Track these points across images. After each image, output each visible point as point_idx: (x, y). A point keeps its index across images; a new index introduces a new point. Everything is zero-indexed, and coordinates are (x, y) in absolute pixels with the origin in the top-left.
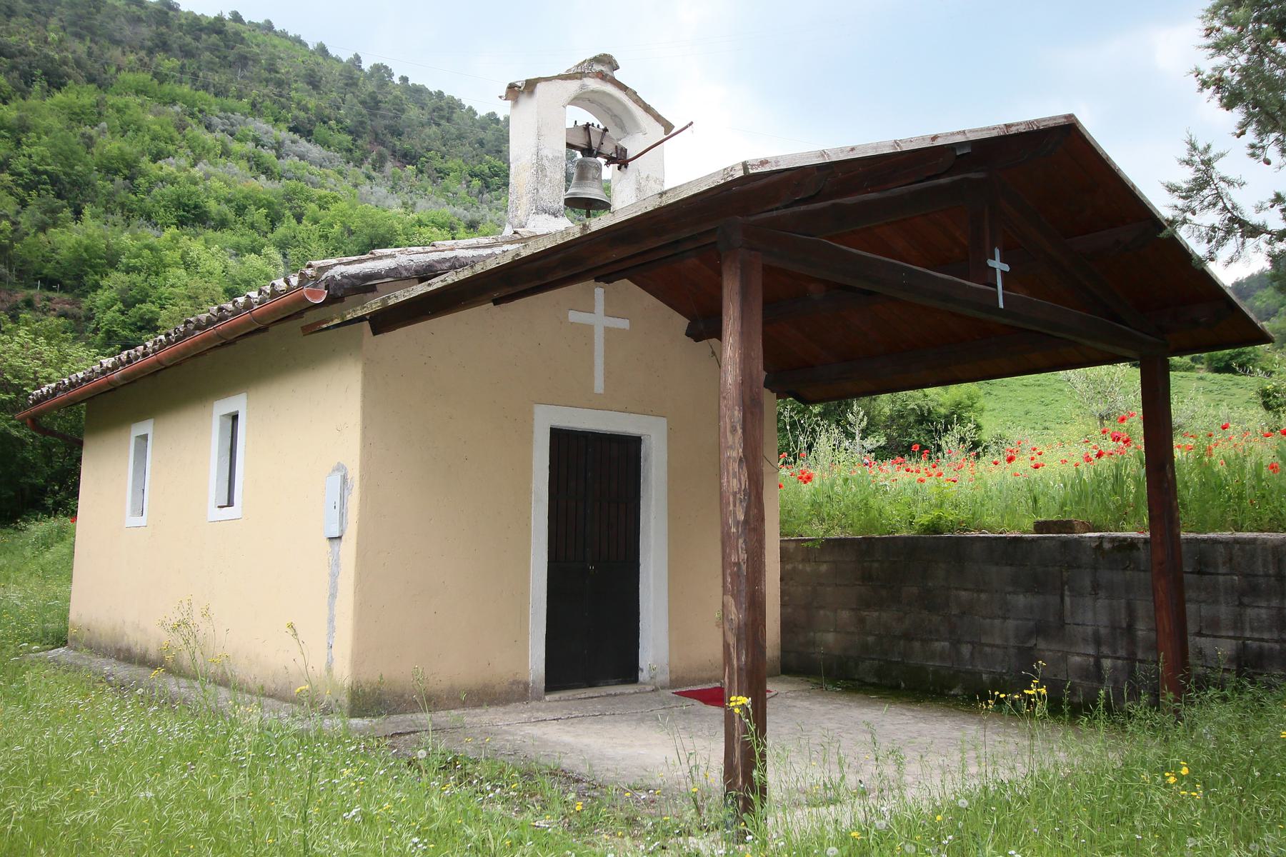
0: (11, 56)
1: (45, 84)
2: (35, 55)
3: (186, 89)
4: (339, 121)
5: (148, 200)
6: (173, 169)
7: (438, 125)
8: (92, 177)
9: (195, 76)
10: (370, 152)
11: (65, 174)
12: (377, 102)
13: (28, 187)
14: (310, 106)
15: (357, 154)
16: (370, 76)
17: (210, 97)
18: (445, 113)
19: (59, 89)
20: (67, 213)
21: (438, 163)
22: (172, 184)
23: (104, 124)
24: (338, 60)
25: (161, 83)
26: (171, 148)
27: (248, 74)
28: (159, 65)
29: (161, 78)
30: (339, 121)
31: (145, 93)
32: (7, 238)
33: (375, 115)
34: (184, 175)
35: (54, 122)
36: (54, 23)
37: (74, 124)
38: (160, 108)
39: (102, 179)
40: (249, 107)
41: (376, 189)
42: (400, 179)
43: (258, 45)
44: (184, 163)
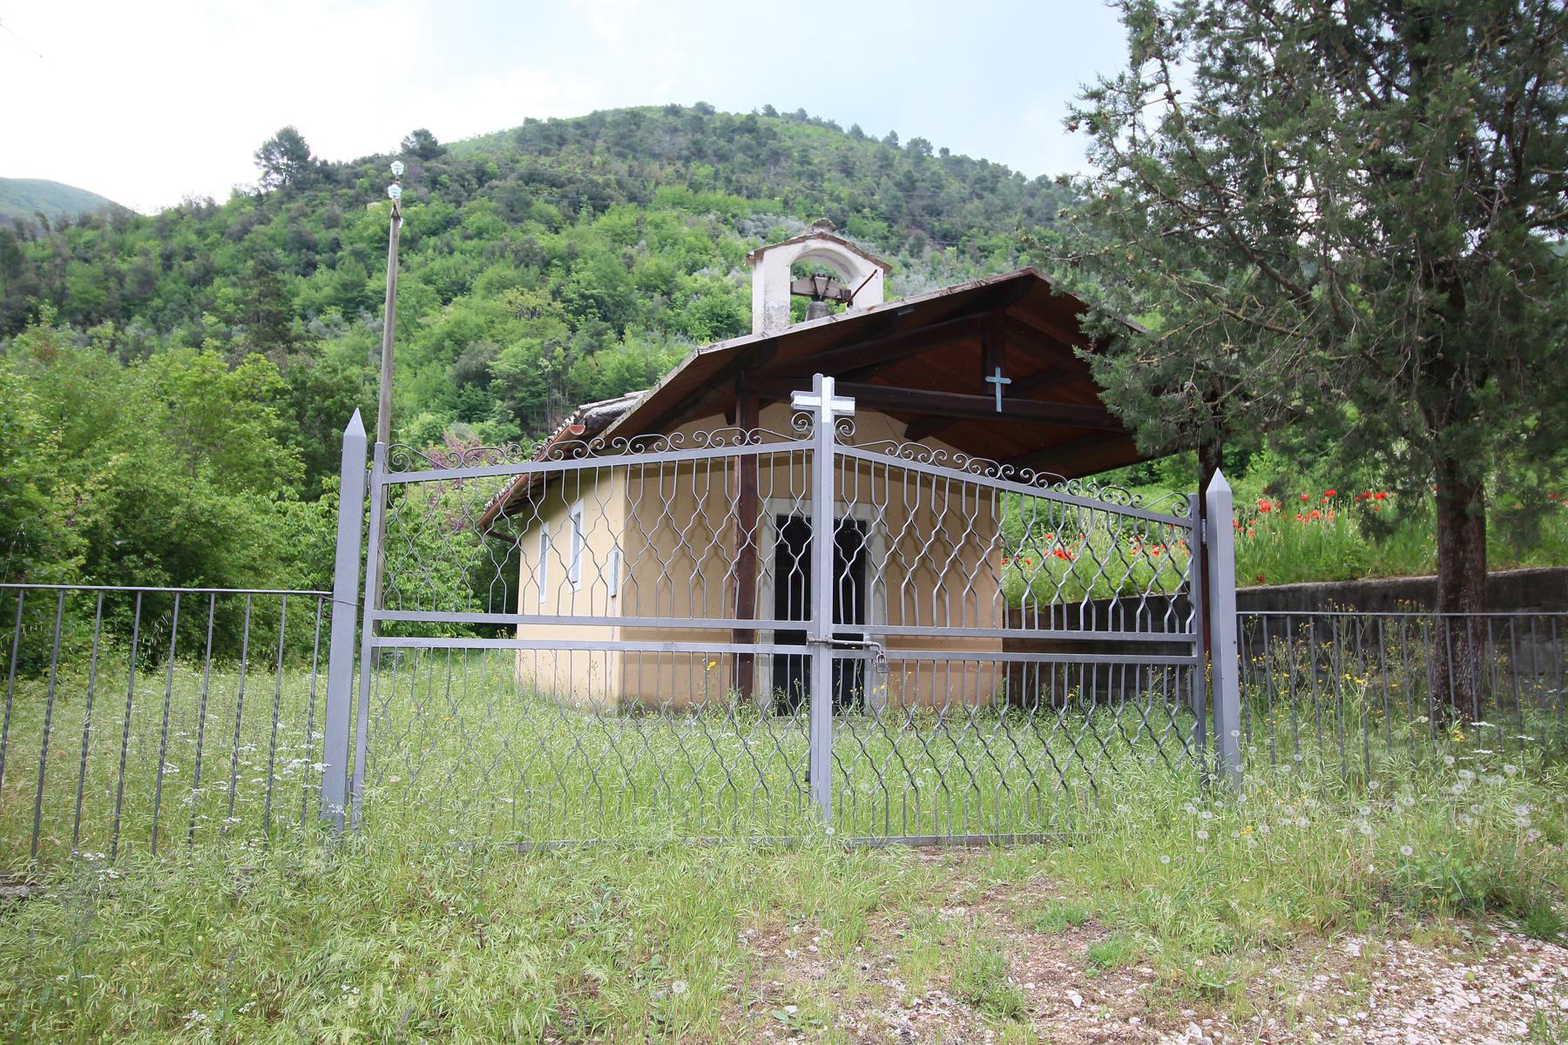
0: (561, 186)
1: (591, 209)
2: (582, 181)
3: (720, 195)
4: (873, 208)
5: (684, 313)
6: (707, 280)
7: (980, 197)
8: (632, 297)
9: (728, 180)
10: (906, 238)
11: (610, 296)
12: (913, 182)
13: (578, 312)
14: (843, 196)
15: (894, 241)
16: (906, 155)
17: (742, 200)
18: (988, 184)
19: (603, 212)
20: (612, 334)
22: (706, 295)
23: (643, 242)
24: (874, 141)
25: (696, 192)
26: (705, 258)
27: (779, 170)
28: (694, 174)
29: (695, 187)
30: (873, 208)
31: (681, 204)
32: (560, 364)
33: (911, 197)
34: (717, 284)
35: (599, 246)
36: (600, 145)
37: (616, 245)
38: (695, 218)
39: (643, 297)
40: (781, 205)
41: (913, 277)
42: (939, 262)
43: (791, 138)
44: (717, 272)
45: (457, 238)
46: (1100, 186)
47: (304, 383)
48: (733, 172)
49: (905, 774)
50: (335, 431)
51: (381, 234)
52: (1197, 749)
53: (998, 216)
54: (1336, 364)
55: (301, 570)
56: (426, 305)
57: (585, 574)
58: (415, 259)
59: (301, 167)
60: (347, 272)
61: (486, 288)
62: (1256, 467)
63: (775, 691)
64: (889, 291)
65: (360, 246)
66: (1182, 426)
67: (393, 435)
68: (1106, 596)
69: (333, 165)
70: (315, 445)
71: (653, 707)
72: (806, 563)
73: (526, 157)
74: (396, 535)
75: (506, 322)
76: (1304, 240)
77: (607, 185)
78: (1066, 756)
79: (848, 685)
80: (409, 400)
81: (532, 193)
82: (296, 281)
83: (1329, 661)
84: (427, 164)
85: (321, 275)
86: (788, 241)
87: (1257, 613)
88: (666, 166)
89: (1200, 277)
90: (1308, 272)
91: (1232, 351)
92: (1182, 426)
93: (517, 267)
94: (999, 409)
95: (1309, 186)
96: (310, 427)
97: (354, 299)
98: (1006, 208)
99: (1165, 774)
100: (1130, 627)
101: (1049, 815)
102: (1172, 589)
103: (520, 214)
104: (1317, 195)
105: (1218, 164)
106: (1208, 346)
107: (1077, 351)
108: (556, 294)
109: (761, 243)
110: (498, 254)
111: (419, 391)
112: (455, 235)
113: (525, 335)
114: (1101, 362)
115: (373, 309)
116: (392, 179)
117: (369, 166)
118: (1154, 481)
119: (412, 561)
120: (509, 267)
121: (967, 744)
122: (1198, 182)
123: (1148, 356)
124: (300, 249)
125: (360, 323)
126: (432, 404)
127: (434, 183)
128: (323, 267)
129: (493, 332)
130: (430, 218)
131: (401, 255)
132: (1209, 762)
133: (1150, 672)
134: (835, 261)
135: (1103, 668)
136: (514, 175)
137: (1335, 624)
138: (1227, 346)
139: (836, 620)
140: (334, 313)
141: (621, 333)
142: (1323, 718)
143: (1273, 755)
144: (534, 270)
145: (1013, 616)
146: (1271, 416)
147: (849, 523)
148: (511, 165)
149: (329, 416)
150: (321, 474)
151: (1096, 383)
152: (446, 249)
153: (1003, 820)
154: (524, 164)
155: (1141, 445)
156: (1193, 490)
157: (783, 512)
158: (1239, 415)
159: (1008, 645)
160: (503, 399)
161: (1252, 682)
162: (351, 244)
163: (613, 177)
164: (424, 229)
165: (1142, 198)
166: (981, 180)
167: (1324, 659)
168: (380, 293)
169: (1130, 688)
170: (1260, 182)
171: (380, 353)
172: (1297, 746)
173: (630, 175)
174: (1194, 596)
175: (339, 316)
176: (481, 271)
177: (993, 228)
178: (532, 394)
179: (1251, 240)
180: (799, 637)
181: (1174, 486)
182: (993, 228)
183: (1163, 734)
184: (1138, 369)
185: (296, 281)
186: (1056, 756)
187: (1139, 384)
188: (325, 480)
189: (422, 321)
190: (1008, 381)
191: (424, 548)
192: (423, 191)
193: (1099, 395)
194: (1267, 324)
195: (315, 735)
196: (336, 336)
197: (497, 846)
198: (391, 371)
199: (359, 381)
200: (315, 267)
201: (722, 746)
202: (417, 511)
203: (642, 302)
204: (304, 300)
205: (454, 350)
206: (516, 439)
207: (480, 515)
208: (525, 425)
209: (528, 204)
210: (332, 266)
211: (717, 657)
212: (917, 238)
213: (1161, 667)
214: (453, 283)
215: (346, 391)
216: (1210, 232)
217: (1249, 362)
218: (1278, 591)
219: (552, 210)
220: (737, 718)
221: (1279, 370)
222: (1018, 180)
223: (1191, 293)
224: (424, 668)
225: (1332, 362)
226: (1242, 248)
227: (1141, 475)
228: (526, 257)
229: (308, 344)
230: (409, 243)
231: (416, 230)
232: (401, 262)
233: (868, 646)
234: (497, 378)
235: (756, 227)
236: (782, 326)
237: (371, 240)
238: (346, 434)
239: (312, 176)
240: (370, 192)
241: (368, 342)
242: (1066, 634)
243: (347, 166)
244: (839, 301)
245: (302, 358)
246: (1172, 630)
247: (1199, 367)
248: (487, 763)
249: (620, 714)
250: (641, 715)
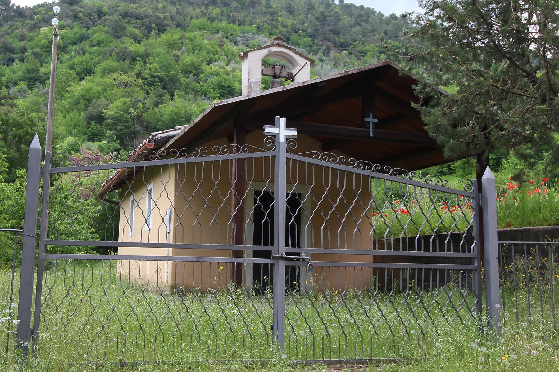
0: (142, 19)
1: (157, 31)
2: (152, 17)
3: (224, 24)
4: (304, 31)
5: (205, 85)
6: (217, 68)
7: (360, 25)
8: (178, 77)
9: (228, 16)
10: (321, 46)
11: (167, 76)
12: (325, 17)
13: (150, 84)
14: (288, 24)
15: (315, 47)
17: (236, 27)
18: (364, 18)
19: (163, 33)
20: (167, 96)
21: (360, 48)
22: (217, 76)
23: (184, 48)
25: (212, 22)
26: (216, 56)
27: (255, 11)
28: (211, 13)
30: (304, 31)
32: (141, 111)
33: (324, 25)
34: (222, 70)
35: (161, 50)
37: (170, 50)
38: (211, 36)
39: (184, 77)
40: (256, 29)
41: (325, 66)
42: (339, 59)
44: (222, 64)
45: (87, 46)
46: (425, 19)
47: (7, 121)
48: (231, 12)
49: (323, 326)
50: (23, 146)
51: (48, 44)
52: (478, 314)
53: (369, 35)
54: (549, 112)
55: (5, 218)
56: (71, 81)
57: (155, 220)
58: (65, 57)
59: (6, 9)
60: (30, 64)
61: (102, 72)
62: (505, 166)
63: (254, 283)
64: (313, 74)
65: (37, 50)
66: (468, 144)
67: (54, 148)
68: (427, 233)
69: (23, 8)
70: (13, 154)
71: (189, 290)
72: (271, 215)
73: (123, 4)
74: (55, 200)
75: (112, 90)
76: (533, 47)
77: (165, 18)
78: (407, 317)
79: (293, 279)
80: (62, 130)
81: (126, 22)
82: (3, 68)
83: (545, 267)
84: (72, 8)
85: (16, 65)
86: (260, 48)
87: (507, 242)
88: (196, 9)
89: (475, 66)
90: (535, 63)
91: (495, 105)
92: (468, 144)
93: (118, 61)
94: (371, 135)
95: (535, 18)
96: (10, 144)
97: (34, 77)
98: (373, 31)
99: (461, 327)
100: (442, 250)
101: (399, 348)
102: (464, 230)
103: (120, 34)
104: (539, 23)
105: (487, 7)
106: (482, 102)
107: (413, 105)
108: (139, 75)
109: (246, 49)
110: (108, 54)
111: (67, 125)
112: (86, 44)
113: (123, 96)
114: (426, 110)
115: (43, 83)
116: (54, 15)
117: (41, 8)
118: (451, 173)
119: (63, 214)
120: (114, 61)
121: (355, 311)
122: (477, 16)
123: (450, 108)
124: (5, 52)
125: (36, 90)
126: (74, 132)
127: (75, 17)
128: (17, 61)
129: (106, 95)
130: (72, 36)
131: (58, 55)
132: (484, 321)
133: (452, 274)
134: (285, 58)
135: (427, 271)
136: (117, 13)
137: (549, 248)
138: (492, 102)
139: (287, 245)
140: (23, 85)
141: (172, 95)
142: (543, 298)
143: (518, 318)
144: (127, 63)
145: (379, 243)
146: (516, 139)
147: (294, 195)
148: (115, 8)
149: (20, 138)
150: (16, 168)
151: (423, 121)
152: (81, 52)
153: (375, 351)
154: (122, 7)
155: (447, 154)
156: (473, 177)
157: (260, 189)
158: (499, 138)
159: (376, 258)
160: (110, 130)
161: (506, 278)
162: (32, 49)
163: (168, 15)
164: (70, 41)
165: (446, 24)
166: (360, 16)
167: (543, 267)
168: (47, 75)
169: (442, 282)
170: (509, 16)
171: (47, 106)
172: (530, 312)
173: (177, 13)
174: (475, 233)
175: (26, 86)
176: (99, 63)
177: (366, 41)
178: (126, 127)
179: (504, 47)
180: (267, 254)
181: (462, 176)
182: (366, 41)
183: (459, 306)
184: (445, 114)
185: (3, 68)
186: (403, 318)
187: (446, 122)
188: (18, 171)
189: (69, 89)
190: (376, 120)
191: (69, 207)
192: (69, 21)
193: (425, 128)
194: (515, 90)
195: (13, 305)
196: (24, 97)
197: (109, 364)
198: (52, 115)
199: (36, 120)
200: (13, 61)
201: (226, 312)
202: (66, 188)
203: (183, 79)
204: (7, 78)
205: (85, 105)
206: (117, 150)
207: (99, 190)
208: (122, 143)
209: (124, 28)
210: (22, 60)
211: (222, 264)
212: (327, 46)
213: (458, 271)
214: (85, 69)
215: (29, 125)
216: (483, 43)
217: (503, 110)
218: (518, 231)
219: (137, 31)
220: (234, 297)
221: (520, 115)
222: (380, 16)
223: (473, 74)
224: (70, 270)
225: (547, 110)
226: (500, 51)
227: (444, 170)
228: (123, 56)
229: (9, 101)
230: (62, 49)
231: (66, 42)
232: (58, 58)
233: (303, 259)
234: (107, 119)
235: (243, 40)
236: (257, 92)
237: (42, 47)
238: (30, 147)
239: (12, 14)
240: (42, 22)
241: (41, 100)
242: (408, 253)
243: (30, 9)
244: (287, 79)
245: (6, 108)
246: (464, 251)
247: (477, 113)
248: (103, 320)
249: (172, 294)
250: (184, 295)
